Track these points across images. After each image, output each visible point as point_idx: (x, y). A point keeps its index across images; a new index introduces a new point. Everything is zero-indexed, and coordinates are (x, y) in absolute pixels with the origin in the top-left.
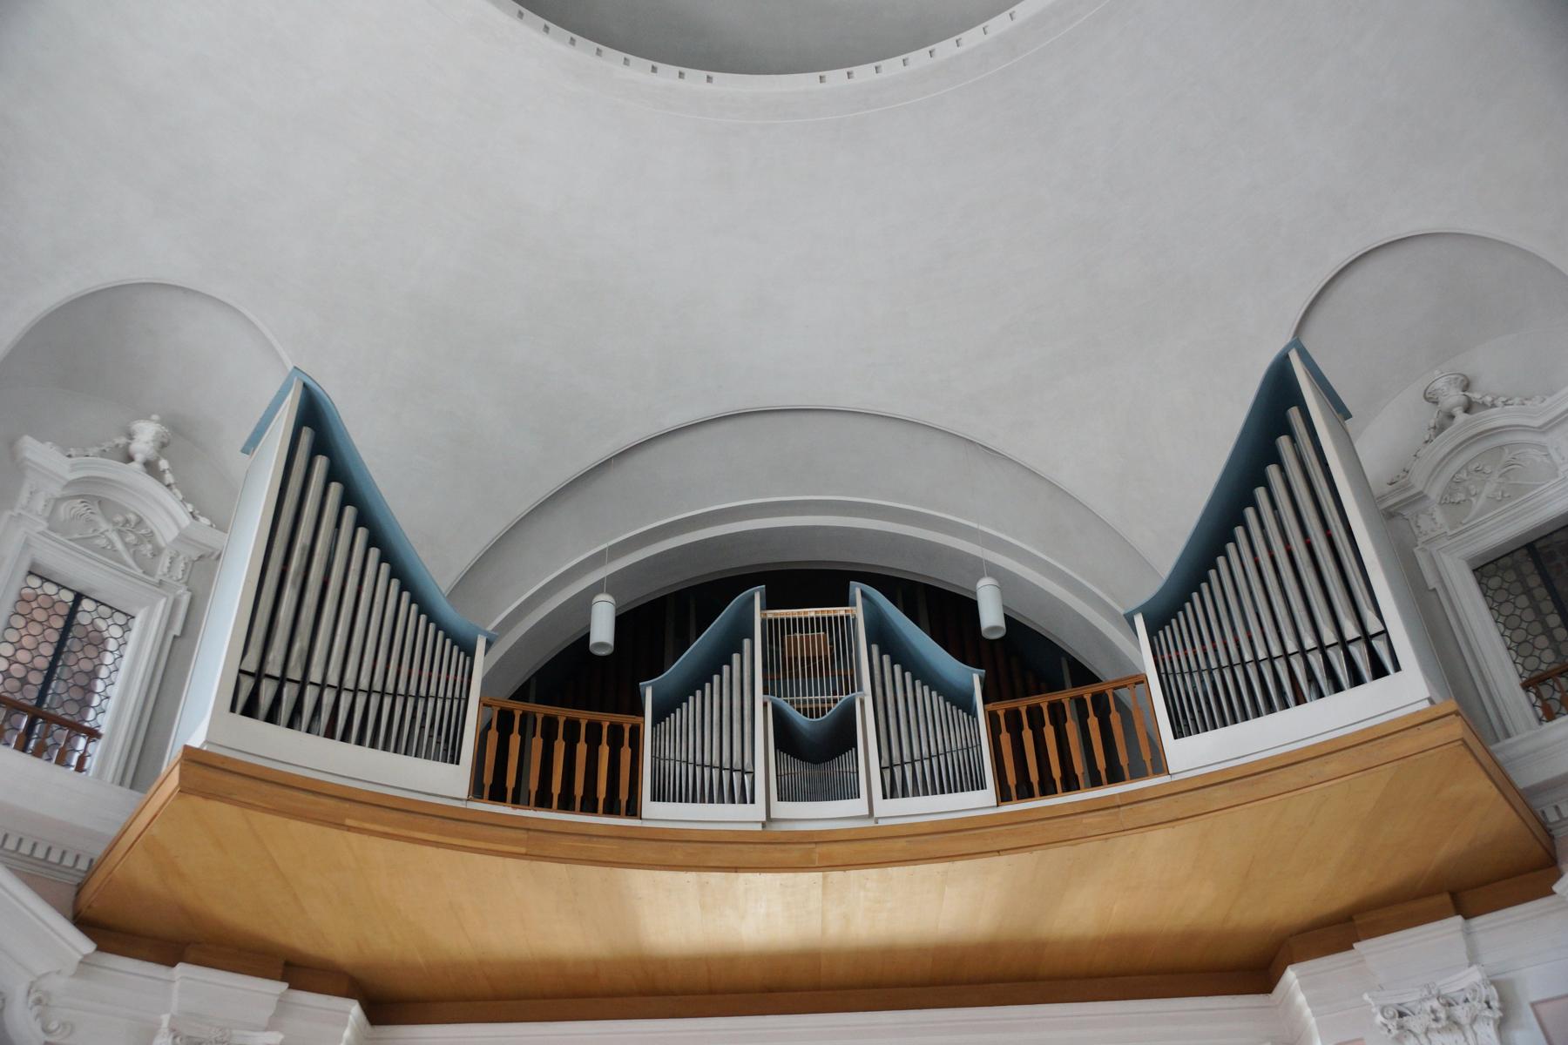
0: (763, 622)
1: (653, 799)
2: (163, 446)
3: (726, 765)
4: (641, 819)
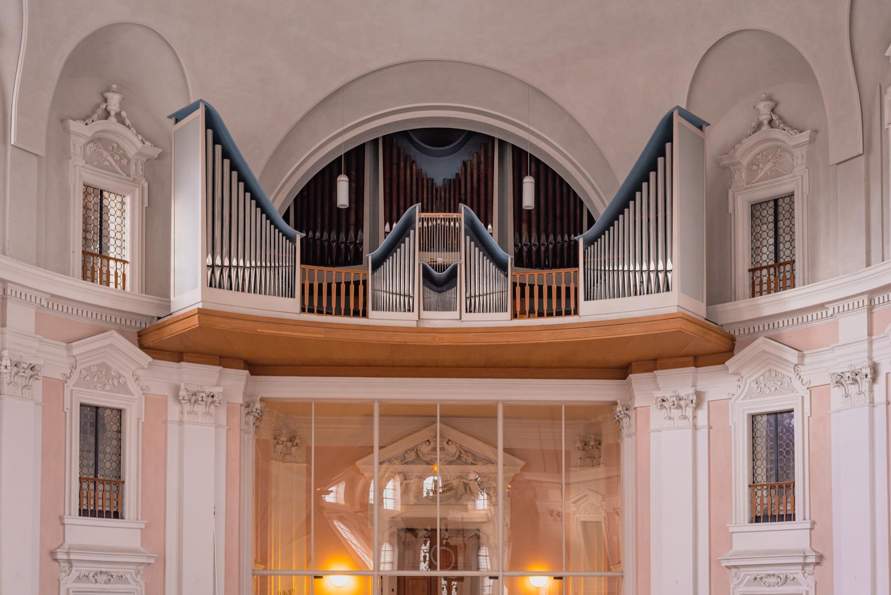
3: (402, 293)
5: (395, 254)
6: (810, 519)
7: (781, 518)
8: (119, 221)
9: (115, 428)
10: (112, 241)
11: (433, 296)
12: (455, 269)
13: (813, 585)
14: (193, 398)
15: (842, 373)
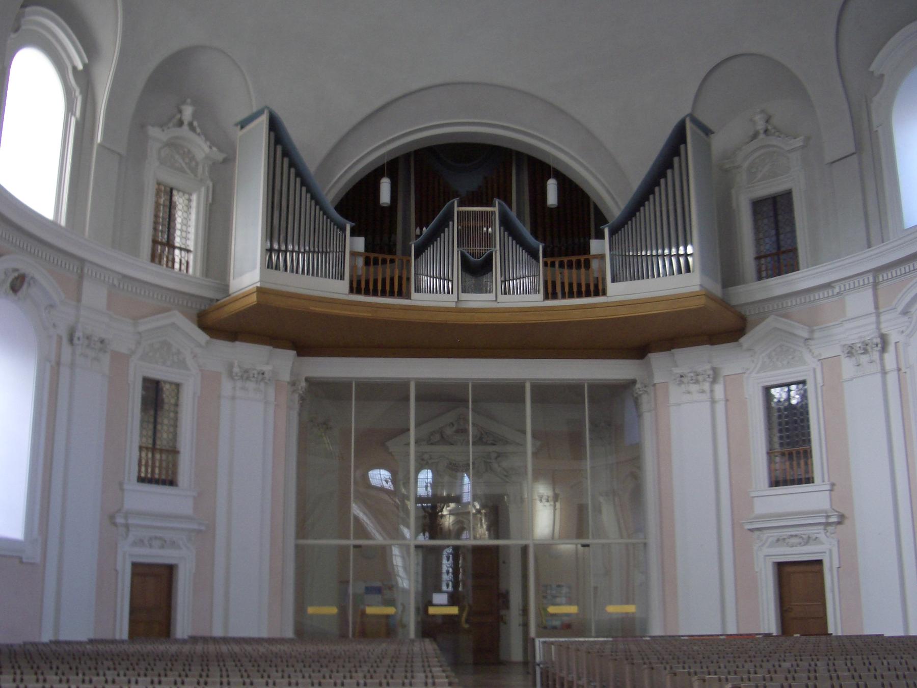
0: (458, 212)
1: (415, 292)
2: (195, 115)
4: (411, 299)
5: (435, 242)
6: (829, 481)
7: (800, 482)
8: (185, 215)
9: (173, 401)
10: (178, 233)
11: (471, 281)
12: (491, 255)
13: (836, 543)
14: (245, 375)
15: (852, 344)
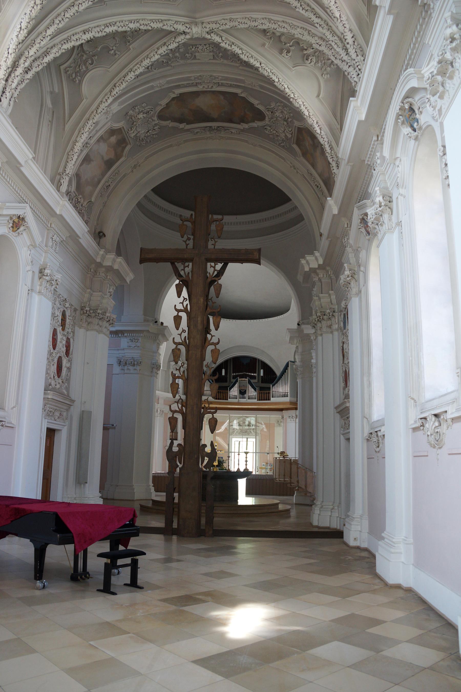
11: (241, 396)
12: (246, 390)
